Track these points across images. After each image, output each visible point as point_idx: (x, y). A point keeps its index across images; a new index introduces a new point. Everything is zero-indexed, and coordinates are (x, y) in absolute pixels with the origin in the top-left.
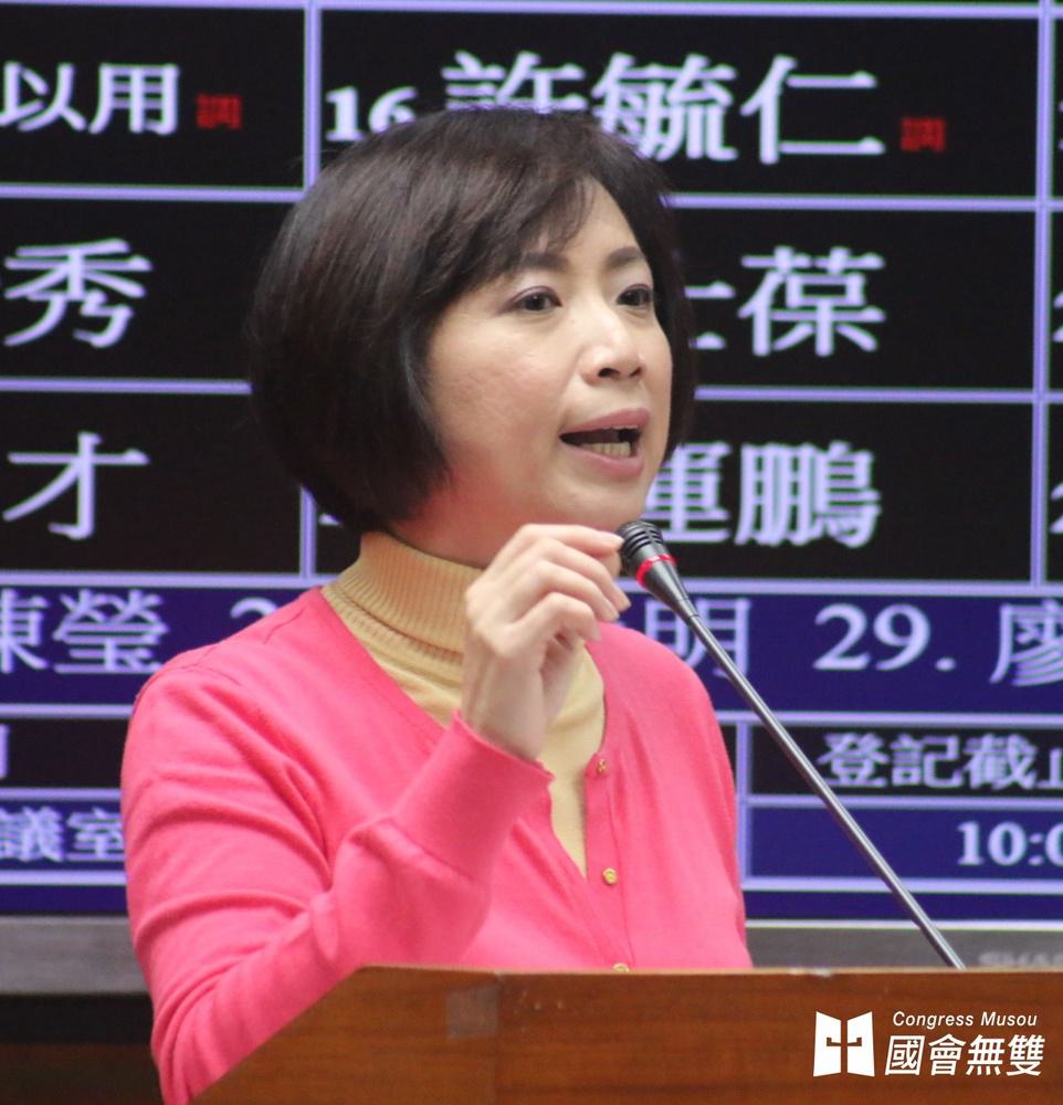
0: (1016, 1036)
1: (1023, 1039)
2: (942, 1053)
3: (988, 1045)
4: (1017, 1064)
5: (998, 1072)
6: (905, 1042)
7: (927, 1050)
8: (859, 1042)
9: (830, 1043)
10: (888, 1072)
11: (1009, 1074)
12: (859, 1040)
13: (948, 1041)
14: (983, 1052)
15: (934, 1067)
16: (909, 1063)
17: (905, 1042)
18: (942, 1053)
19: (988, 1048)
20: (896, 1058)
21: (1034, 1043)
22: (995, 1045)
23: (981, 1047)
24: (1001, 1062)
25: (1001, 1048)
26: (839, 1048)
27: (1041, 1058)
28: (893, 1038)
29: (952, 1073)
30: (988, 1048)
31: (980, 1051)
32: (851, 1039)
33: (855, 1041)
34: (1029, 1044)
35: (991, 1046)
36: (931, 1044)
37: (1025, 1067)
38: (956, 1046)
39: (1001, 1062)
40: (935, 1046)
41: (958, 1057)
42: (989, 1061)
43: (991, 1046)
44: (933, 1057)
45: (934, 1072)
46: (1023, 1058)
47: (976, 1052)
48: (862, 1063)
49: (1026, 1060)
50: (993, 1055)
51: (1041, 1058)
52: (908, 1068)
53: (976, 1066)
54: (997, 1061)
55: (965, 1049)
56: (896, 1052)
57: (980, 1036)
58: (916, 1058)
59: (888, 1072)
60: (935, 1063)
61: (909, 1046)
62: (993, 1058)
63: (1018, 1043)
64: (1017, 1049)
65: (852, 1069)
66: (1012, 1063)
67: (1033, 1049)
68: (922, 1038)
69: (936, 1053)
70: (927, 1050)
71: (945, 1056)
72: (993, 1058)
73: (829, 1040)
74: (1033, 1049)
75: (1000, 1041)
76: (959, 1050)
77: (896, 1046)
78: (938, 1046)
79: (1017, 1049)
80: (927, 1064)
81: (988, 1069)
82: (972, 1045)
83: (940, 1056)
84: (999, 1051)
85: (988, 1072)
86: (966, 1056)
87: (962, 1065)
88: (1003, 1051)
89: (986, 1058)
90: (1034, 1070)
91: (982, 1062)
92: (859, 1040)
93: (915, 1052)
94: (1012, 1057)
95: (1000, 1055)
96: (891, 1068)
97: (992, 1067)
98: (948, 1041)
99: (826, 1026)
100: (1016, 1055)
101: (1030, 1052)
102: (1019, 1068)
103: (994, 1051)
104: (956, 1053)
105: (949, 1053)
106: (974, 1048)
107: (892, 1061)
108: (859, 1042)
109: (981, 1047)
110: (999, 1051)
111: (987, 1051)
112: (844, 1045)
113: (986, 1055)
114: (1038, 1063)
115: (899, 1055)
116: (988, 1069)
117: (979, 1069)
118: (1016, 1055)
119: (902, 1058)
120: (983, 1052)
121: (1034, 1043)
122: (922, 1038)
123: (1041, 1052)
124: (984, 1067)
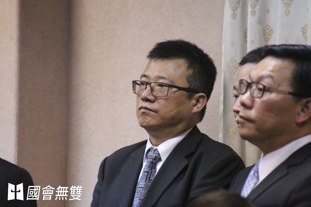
0: (72, 186)
1: (75, 187)
3: (63, 189)
5: (66, 199)
6: (33, 188)
7: (41, 191)
8: (19, 191)
9: (12, 191)
10: (28, 199)
11: (70, 200)
12: (20, 190)
13: (49, 188)
14: (61, 192)
15: (44, 197)
16: (35, 196)
17: (33, 188)
18: (47, 192)
19: (62, 190)
20: (30, 194)
22: (65, 189)
23: (60, 190)
24: (67, 195)
26: (14, 193)
27: (81, 194)
28: (29, 187)
29: (50, 199)
30: (62, 190)
31: (60, 192)
32: (17, 190)
33: (19, 191)
34: (77, 189)
36: (43, 189)
38: (52, 189)
39: (67, 195)
40: (44, 190)
41: (52, 194)
42: (63, 195)
43: (64, 190)
44: (43, 193)
45: (44, 199)
46: (75, 194)
47: (58, 192)
48: (20, 197)
49: (76, 195)
50: (65, 193)
51: (81, 194)
52: (35, 198)
53: (58, 197)
54: (66, 195)
55: (55, 191)
56: (31, 192)
57: (60, 186)
58: (37, 194)
59: (28, 199)
60: (44, 196)
62: (64, 194)
63: (73, 189)
64: (73, 191)
65: (17, 199)
66: (71, 196)
68: (40, 187)
69: (44, 192)
70: (41, 191)
71: (48, 193)
72: (64, 194)
73: (12, 190)
75: (67, 188)
76: (52, 191)
77: (31, 190)
78: (45, 189)
79: (73, 191)
80: (41, 196)
81: (63, 197)
82: (57, 189)
83: (46, 193)
84: (66, 191)
85: (63, 199)
86: (55, 193)
87: (54, 196)
88: (68, 192)
89: (62, 194)
91: (61, 195)
92: (20, 190)
93: (37, 192)
94: (71, 194)
95: (67, 193)
96: (29, 198)
97: (64, 197)
98: (49, 188)
99: (11, 187)
100: (72, 193)
101: (77, 192)
102: (73, 197)
103: (65, 192)
104: (51, 192)
105: (49, 192)
106: (58, 190)
108: (19, 191)
109: (60, 190)
111: (62, 192)
112: (16, 192)
113: (62, 193)
114: (80, 196)
115: (31, 193)
116: (63, 197)
117: (60, 197)
118: (72, 193)
119: (32, 194)
120: (61, 192)
122: (40, 187)
123: (81, 190)
124: (61, 197)
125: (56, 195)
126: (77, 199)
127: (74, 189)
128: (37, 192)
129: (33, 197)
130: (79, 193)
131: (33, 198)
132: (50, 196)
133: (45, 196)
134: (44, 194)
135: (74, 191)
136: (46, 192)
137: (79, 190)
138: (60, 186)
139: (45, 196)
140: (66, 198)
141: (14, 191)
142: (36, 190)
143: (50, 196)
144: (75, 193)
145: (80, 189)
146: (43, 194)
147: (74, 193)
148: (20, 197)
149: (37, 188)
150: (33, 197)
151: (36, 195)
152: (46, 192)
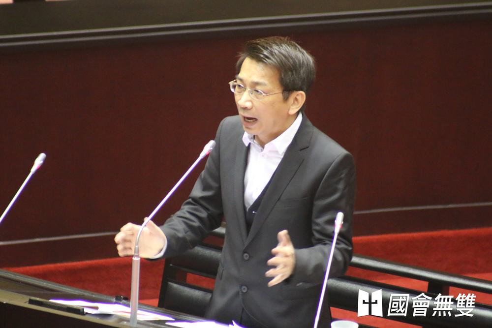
0: (460, 294)
1: (464, 296)
2: (419, 304)
3: (444, 299)
4: (461, 310)
5: (450, 314)
8: (376, 302)
9: (364, 302)
10: (389, 314)
11: (456, 316)
12: (376, 301)
13: (422, 297)
14: (442, 302)
15: (415, 312)
16: (400, 309)
18: (419, 304)
20: (393, 307)
21: (470, 298)
22: (448, 299)
25: (452, 301)
26: (368, 304)
29: (425, 315)
31: (440, 303)
32: (373, 301)
34: (467, 298)
35: (446, 300)
37: (465, 312)
40: (415, 300)
42: (445, 309)
43: (446, 300)
45: (414, 315)
46: (464, 307)
51: (474, 307)
52: (400, 312)
56: (394, 303)
57: (440, 294)
58: (405, 307)
60: (415, 309)
61: (400, 300)
64: (460, 302)
67: (470, 301)
69: (416, 304)
71: (421, 306)
73: (364, 301)
74: (470, 301)
75: (451, 297)
79: (460, 302)
81: (444, 313)
82: (436, 299)
83: (418, 306)
85: (445, 315)
87: (430, 310)
90: (470, 313)
91: (441, 309)
92: (376, 301)
93: (404, 303)
96: (391, 312)
97: (447, 312)
98: (422, 297)
100: (460, 305)
101: (468, 303)
107: (392, 308)
108: (376, 302)
110: (450, 303)
112: (370, 303)
115: (395, 305)
116: (444, 313)
117: (440, 312)
119: (397, 306)
121: (470, 298)
123: (474, 300)
124: (442, 312)
125: (434, 309)
126: (467, 314)
127: (463, 298)
128: (404, 303)
129: (397, 312)
130: (471, 305)
131: (398, 313)
132: (424, 310)
133: (417, 311)
134: (415, 308)
135: (462, 302)
136: (417, 304)
137: (470, 300)
138: (440, 294)
139: (417, 311)
140: (449, 313)
141: (368, 302)
142: (403, 300)
143: (424, 310)
144: (463, 305)
145: (472, 298)
146: (413, 307)
147: (462, 305)
148: (377, 310)
149: (404, 297)
150: (397, 312)
151: (403, 309)
152: (417, 304)
